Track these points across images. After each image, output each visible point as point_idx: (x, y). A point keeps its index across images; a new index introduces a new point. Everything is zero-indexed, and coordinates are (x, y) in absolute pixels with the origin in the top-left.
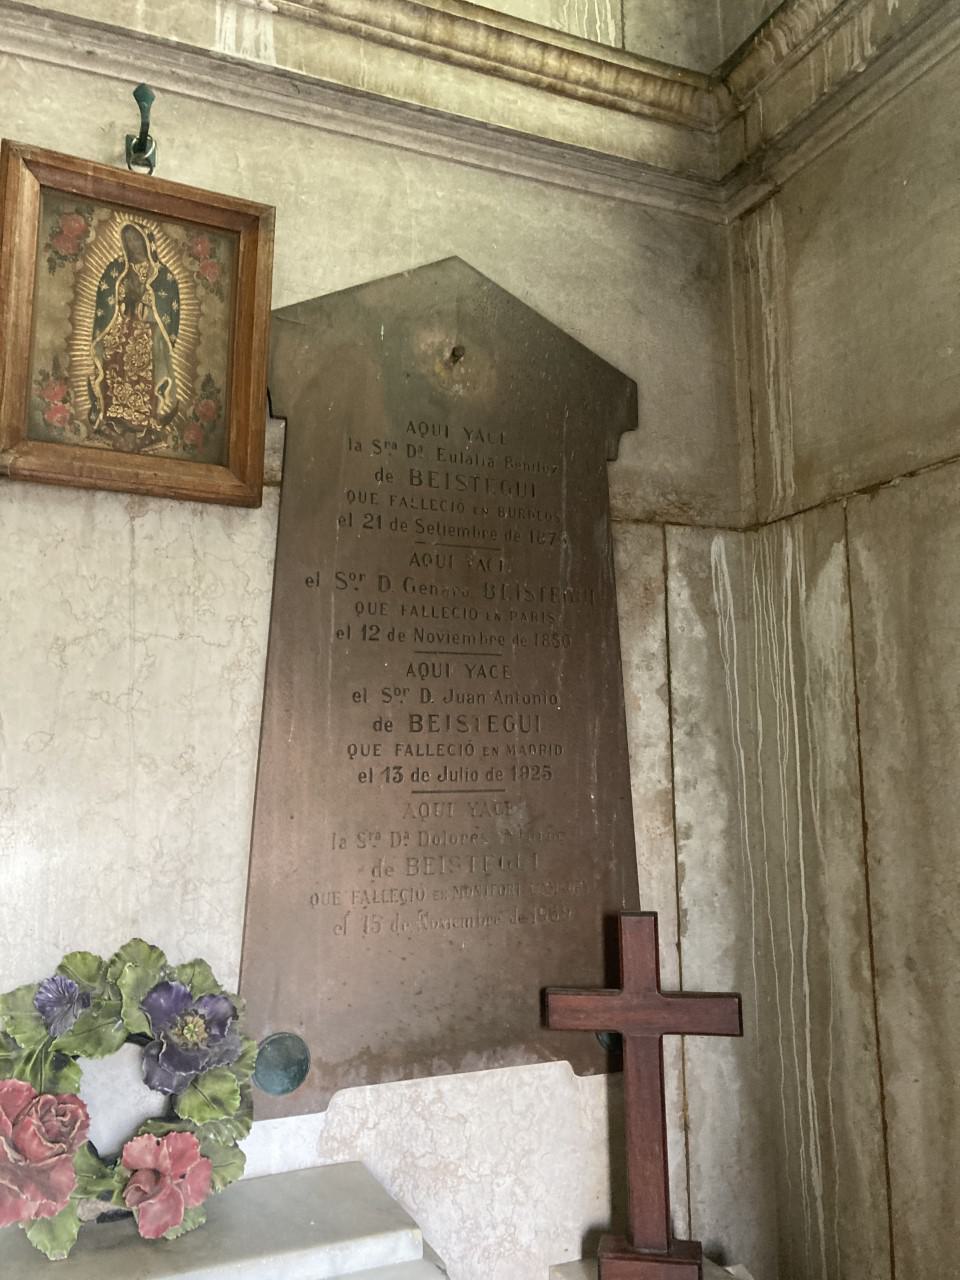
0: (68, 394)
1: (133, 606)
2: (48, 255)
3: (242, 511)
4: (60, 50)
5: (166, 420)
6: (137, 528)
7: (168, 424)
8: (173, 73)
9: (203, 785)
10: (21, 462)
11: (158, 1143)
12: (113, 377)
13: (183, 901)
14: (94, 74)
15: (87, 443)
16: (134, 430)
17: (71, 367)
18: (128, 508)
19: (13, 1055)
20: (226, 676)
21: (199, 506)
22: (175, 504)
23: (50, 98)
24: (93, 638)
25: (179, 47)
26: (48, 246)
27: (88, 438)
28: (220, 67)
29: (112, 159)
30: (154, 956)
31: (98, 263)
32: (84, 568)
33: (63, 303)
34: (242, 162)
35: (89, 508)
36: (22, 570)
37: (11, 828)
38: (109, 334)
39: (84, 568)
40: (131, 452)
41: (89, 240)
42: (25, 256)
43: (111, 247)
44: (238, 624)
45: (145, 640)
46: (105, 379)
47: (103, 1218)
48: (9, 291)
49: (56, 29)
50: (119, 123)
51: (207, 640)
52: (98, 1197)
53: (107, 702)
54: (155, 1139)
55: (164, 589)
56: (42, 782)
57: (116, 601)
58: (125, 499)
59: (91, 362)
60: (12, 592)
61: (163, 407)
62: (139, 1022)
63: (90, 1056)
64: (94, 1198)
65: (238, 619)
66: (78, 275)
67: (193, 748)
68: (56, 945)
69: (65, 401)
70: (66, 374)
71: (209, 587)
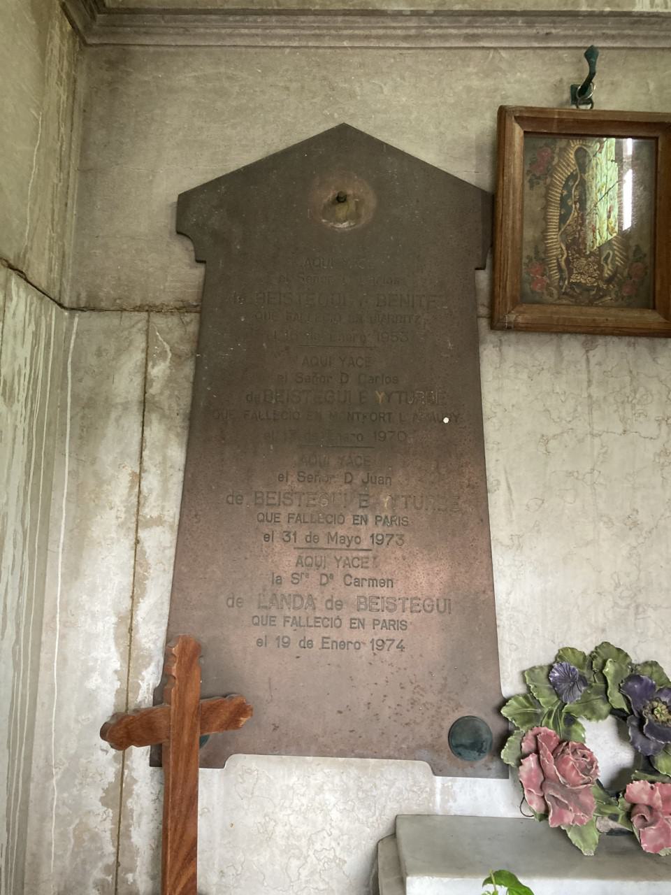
0: (545, 270)
1: (590, 413)
2: (529, 178)
3: (663, 341)
4: (528, 37)
5: (609, 281)
6: (591, 358)
7: (611, 283)
8: (604, 34)
9: (645, 538)
10: (520, 320)
11: (652, 788)
12: (573, 255)
13: (636, 619)
14: (549, 48)
15: (558, 302)
16: (588, 290)
17: (546, 251)
18: (584, 344)
19: (539, 711)
20: (657, 461)
21: (632, 339)
22: (615, 339)
23: (520, 72)
24: (565, 435)
25: (612, 14)
26: (529, 172)
27: (559, 298)
28: (636, 22)
29: (562, 104)
30: (621, 656)
31: (560, 178)
32: (558, 387)
33: (539, 209)
34: (652, 86)
35: (559, 347)
36: (518, 390)
37: (521, 561)
38: (569, 225)
39: (558, 387)
40: (587, 305)
41: (554, 163)
42: (517, 180)
43: (569, 165)
44: (664, 422)
45: (600, 435)
46: (568, 256)
47: (612, 832)
48: (509, 206)
49: (527, 23)
50: (565, 78)
51: (642, 435)
52: (609, 817)
53: (577, 478)
54: (649, 785)
55: (611, 399)
56: (538, 531)
57: (579, 408)
58: (582, 338)
59: (558, 246)
60: (513, 406)
61: (607, 273)
62: (618, 701)
63: (589, 719)
64: (606, 818)
65: (663, 419)
66: (548, 188)
67: (637, 511)
68: (553, 642)
69: (543, 275)
70: (543, 256)
71: (642, 397)
